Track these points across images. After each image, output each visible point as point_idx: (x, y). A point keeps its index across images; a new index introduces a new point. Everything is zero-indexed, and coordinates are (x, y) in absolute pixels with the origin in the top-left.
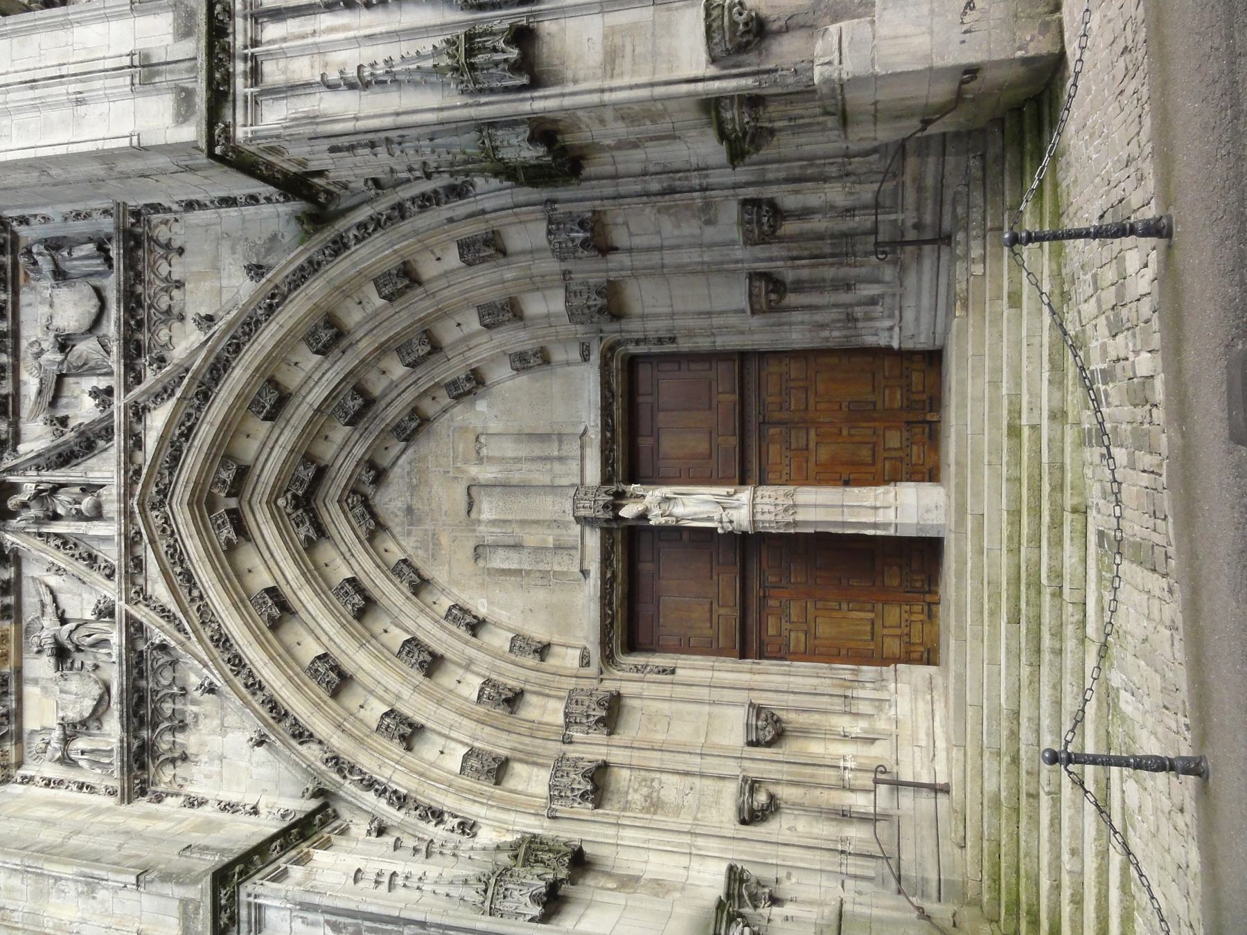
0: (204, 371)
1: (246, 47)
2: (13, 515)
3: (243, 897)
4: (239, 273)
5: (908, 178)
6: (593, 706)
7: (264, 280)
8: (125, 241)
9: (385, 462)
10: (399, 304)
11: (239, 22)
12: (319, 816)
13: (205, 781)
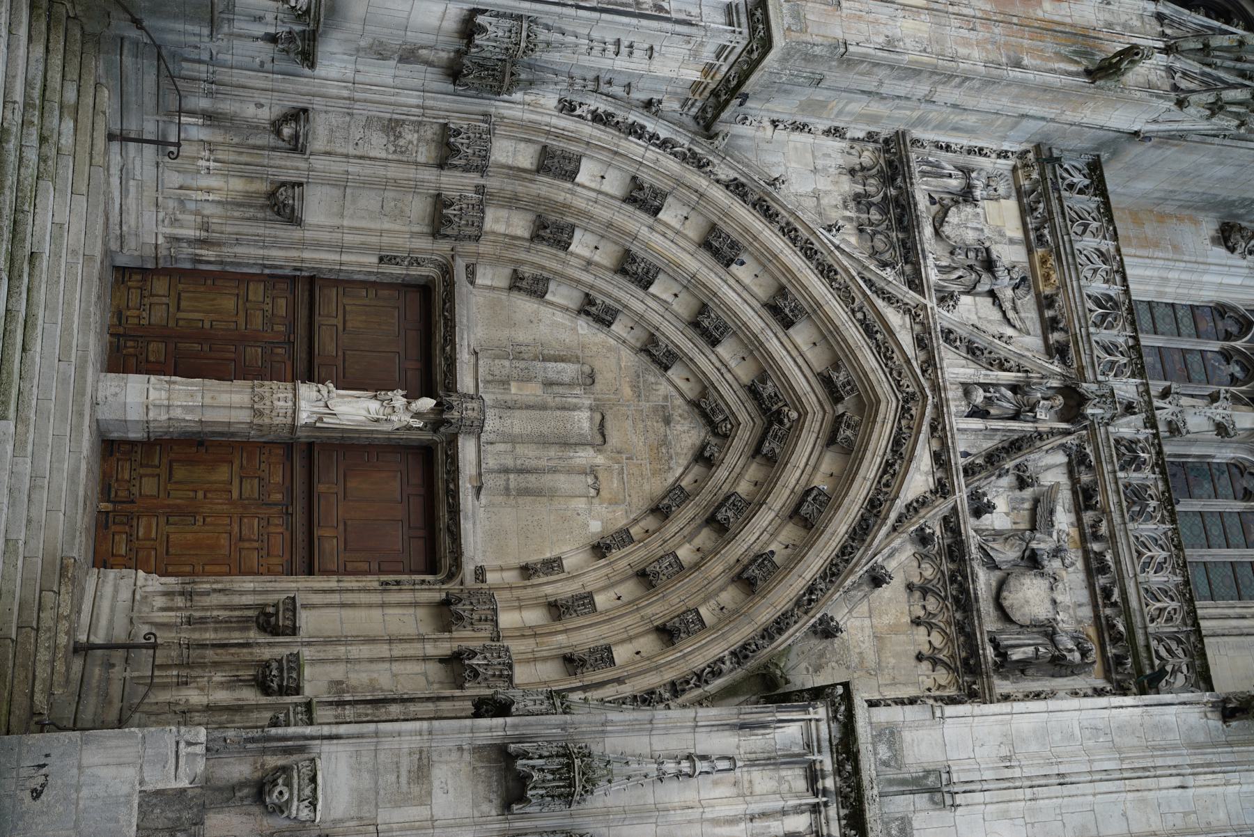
0: (876, 528)
1: (826, 804)
2: (1059, 391)
4: (853, 632)
5: (117, 705)
7: (818, 616)
8: (978, 664)
13: (830, 151)
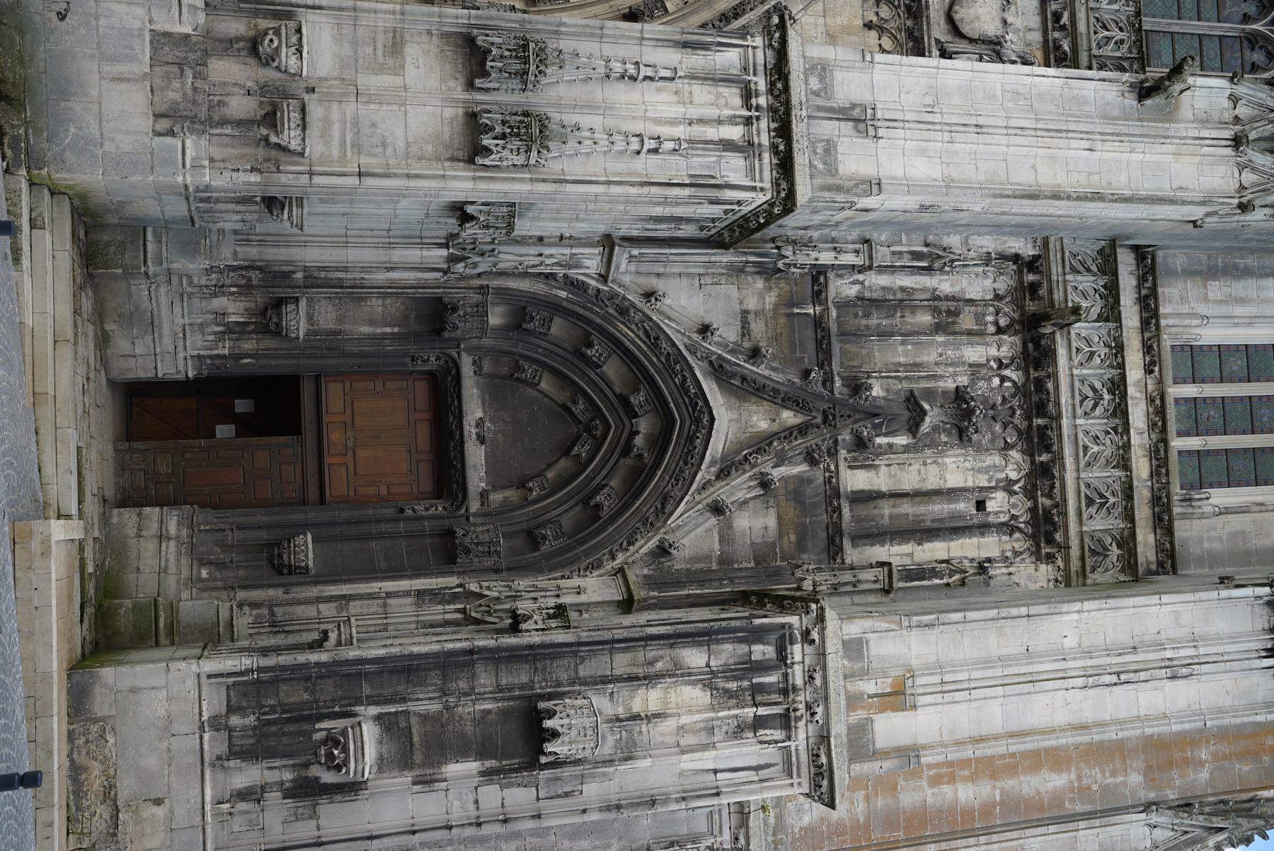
4: (806, 27)
11: (765, 140)
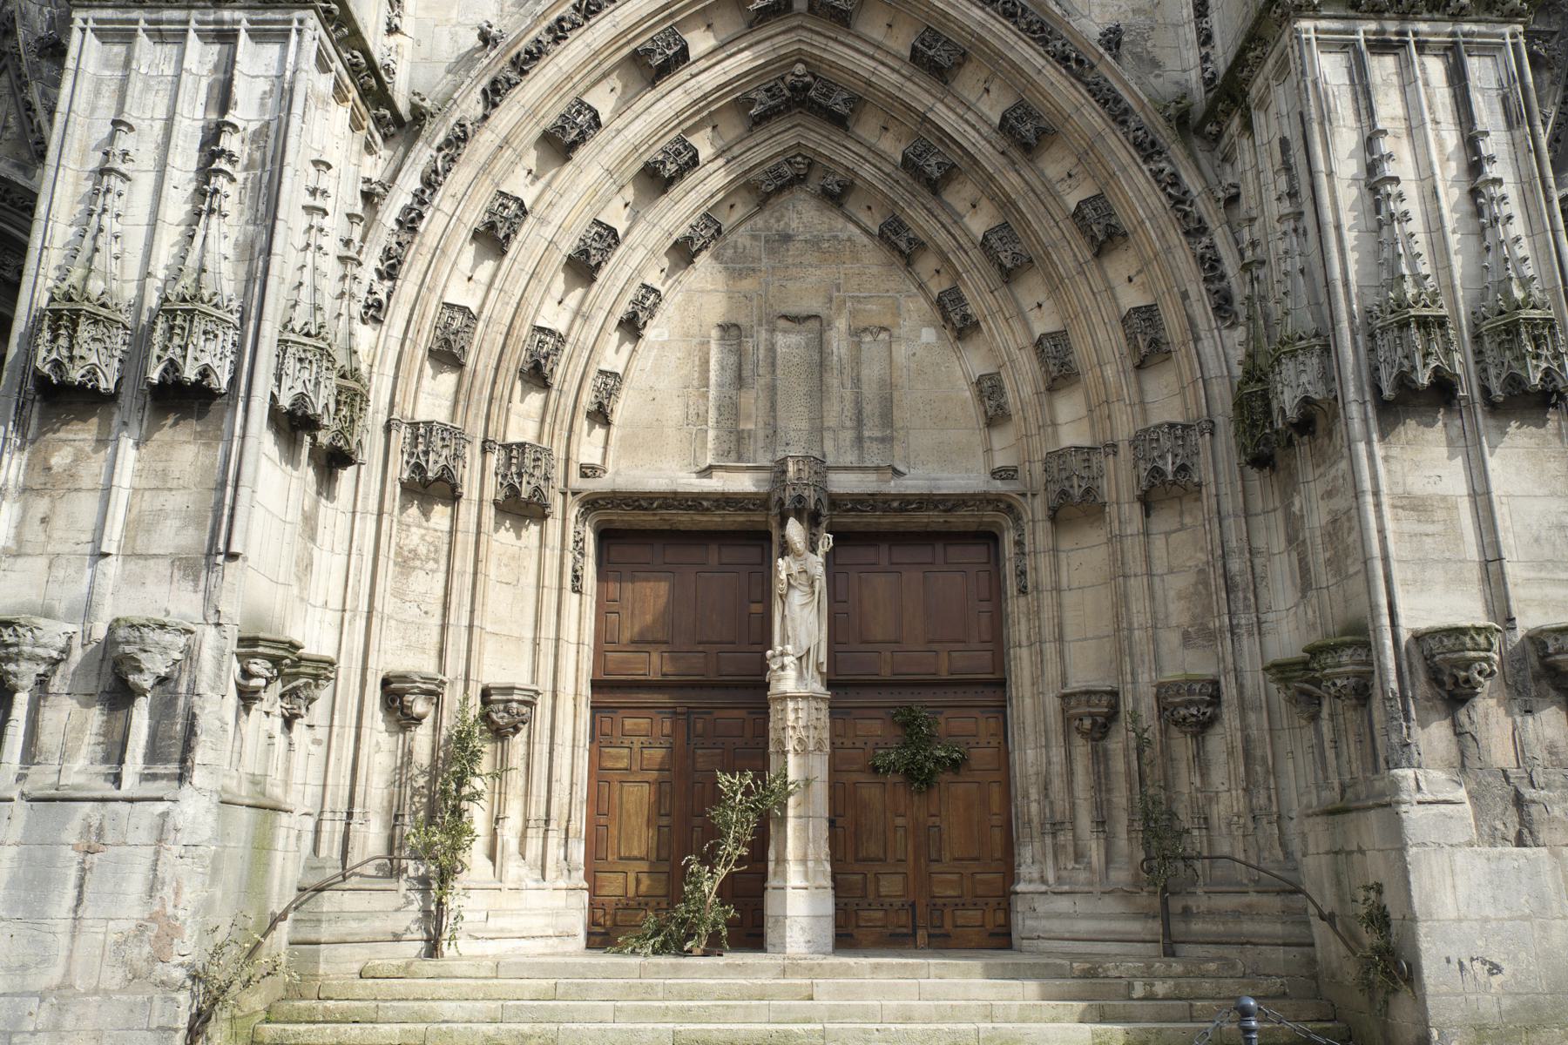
1: (1415, 34)
3: (297, 14)
4: (1108, 17)
5: (1253, 898)
6: (533, 481)
7: (1101, 50)
9: (853, 205)
10: (1068, 227)
11: (1449, 28)
12: (388, 113)
